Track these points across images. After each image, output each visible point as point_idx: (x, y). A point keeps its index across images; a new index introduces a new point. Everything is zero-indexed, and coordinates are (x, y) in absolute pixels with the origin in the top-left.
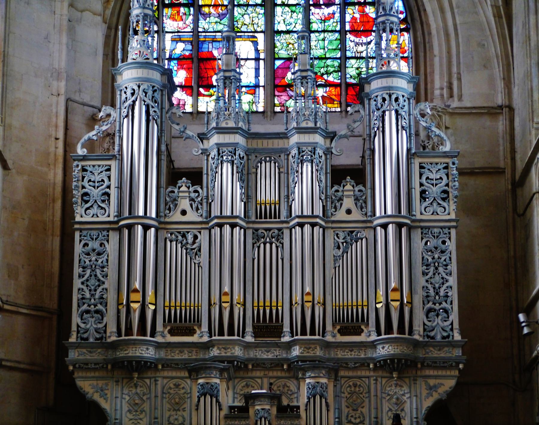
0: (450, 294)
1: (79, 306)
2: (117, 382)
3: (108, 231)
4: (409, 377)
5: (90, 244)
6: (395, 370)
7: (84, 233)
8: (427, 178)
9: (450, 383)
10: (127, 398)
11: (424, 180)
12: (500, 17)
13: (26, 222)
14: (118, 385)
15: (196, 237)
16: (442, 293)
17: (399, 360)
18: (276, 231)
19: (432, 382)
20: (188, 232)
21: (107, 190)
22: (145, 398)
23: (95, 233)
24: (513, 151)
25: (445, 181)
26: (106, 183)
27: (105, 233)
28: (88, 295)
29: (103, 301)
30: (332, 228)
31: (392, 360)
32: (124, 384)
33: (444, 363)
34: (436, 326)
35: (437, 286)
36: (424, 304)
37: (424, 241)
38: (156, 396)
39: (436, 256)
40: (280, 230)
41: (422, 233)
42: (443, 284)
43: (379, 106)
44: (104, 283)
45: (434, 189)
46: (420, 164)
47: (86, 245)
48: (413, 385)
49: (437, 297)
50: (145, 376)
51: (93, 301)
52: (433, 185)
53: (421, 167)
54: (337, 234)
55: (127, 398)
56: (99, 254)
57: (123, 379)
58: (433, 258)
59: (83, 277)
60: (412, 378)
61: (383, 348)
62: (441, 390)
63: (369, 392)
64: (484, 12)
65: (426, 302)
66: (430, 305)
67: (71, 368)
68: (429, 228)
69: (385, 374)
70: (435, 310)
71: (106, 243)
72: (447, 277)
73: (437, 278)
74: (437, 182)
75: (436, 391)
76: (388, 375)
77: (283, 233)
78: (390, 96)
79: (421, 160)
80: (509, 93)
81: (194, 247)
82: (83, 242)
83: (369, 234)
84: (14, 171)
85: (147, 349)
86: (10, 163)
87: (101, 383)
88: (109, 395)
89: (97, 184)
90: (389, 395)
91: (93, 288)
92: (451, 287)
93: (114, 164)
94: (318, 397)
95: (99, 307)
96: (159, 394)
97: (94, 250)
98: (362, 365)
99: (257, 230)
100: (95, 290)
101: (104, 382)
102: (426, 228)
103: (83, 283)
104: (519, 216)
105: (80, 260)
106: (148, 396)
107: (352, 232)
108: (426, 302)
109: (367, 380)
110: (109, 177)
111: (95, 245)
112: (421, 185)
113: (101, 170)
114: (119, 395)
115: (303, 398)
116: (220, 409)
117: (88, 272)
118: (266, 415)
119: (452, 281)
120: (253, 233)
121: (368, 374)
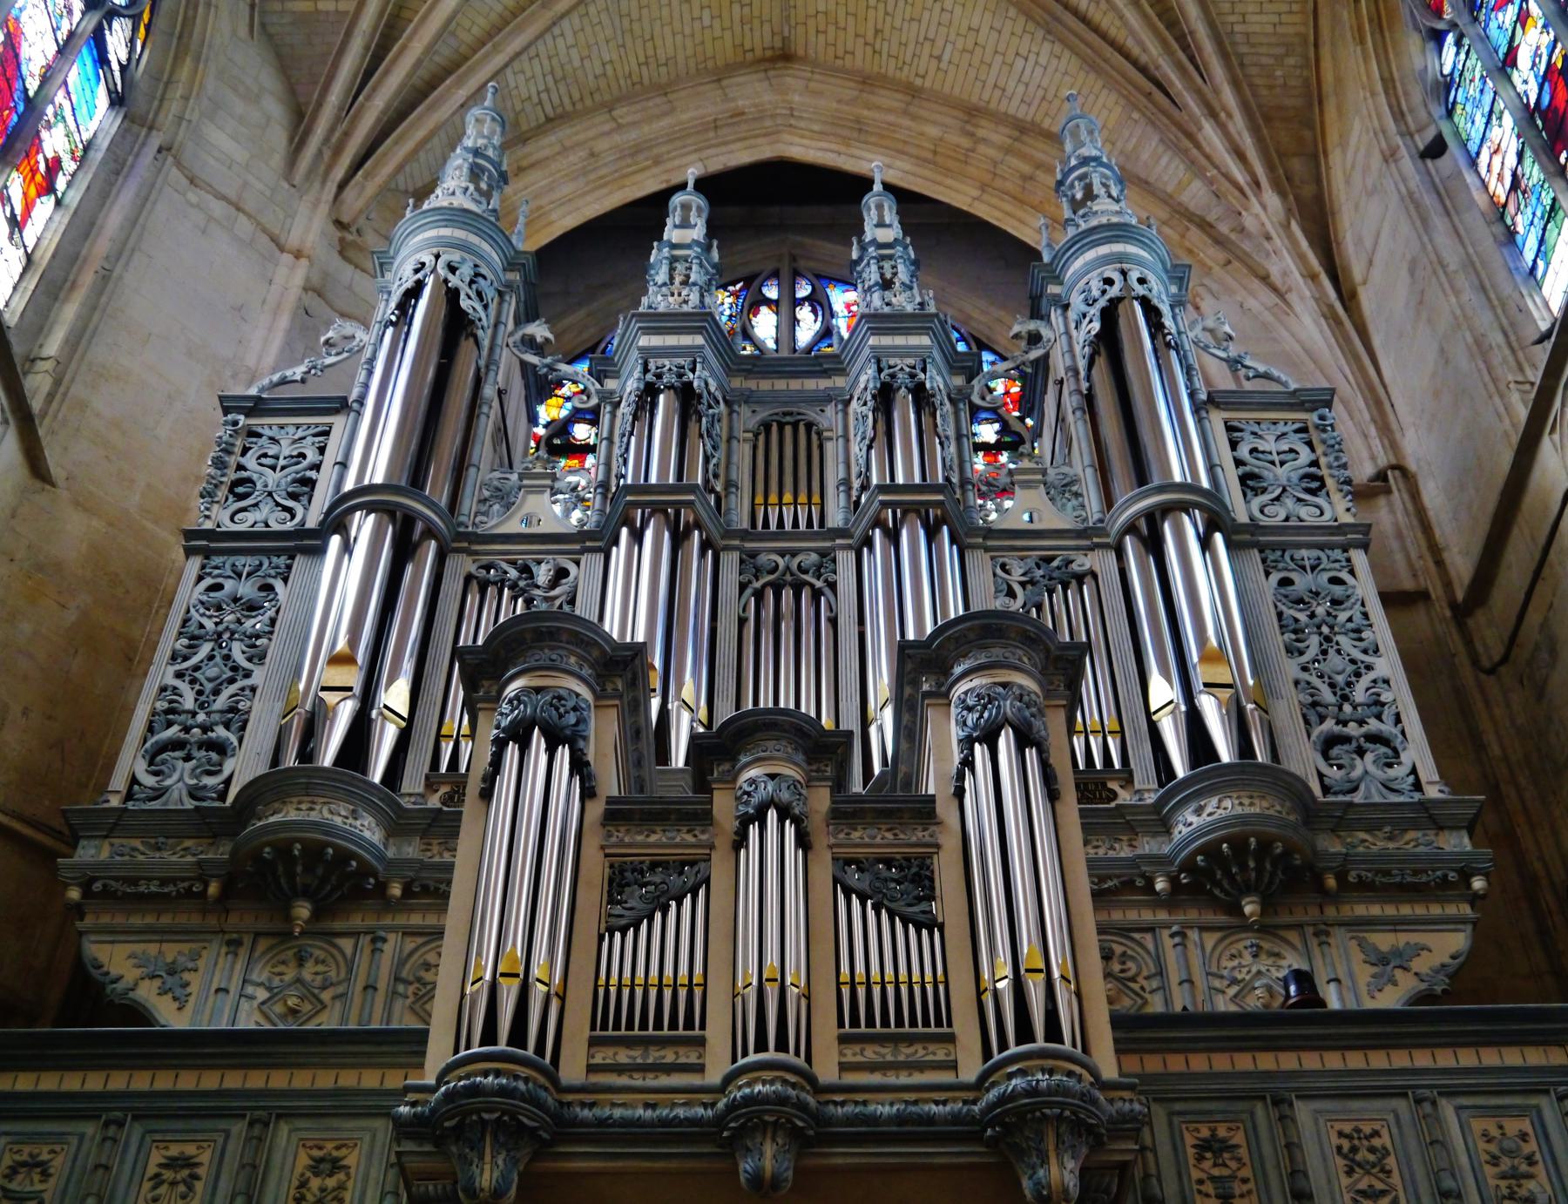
0: (1386, 697)
1: (151, 729)
2: (234, 945)
3: (292, 558)
4: (1299, 927)
5: (229, 585)
6: (1247, 889)
7: (217, 560)
8: (1253, 451)
9: (1450, 945)
10: (262, 994)
11: (1243, 451)
12: (1338, 322)
13: (71, 616)
14: (236, 955)
15: (561, 573)
16: (1359, 695)
17: (1265, 845)
18: (814, 557)
19: (1384, 941)
20: (539, 562)
21: (312, 474)
22: (326, 996)
23: (246, 563)
24: (1435, 550)
25: (1305, 455)
26: (312, 456)
27: (282, 561)
28: (189, 702)
29: (236, 718)
30: (987, 549)
31: (1239, 843)
32: (257, 954)
33: (1416, 873)
34: (1361, 779)
35: (1340, 679)
36: (1307, 722)
37: (1275, 577)
38: (370, 987)
39: (1320, 611)
40: (823, 554)
41: (1264, 561)
42: (1358, 675)
43: (1096, 293)
44: (248, 674)
45: (1279, 471)
46: (1226, 423)
47: (218, 587)
48: (1316, 951)
49: (1347, 708)
50: (338, 925)
51: (201, 717)
52: (1273, 463)
53: (1230, 429)
54: (1003, 567)
55: (262, 994)
56: (252, 608)
57: (257, 935)
58: (1312, 616)
59: (186, 659)
60: (1310, 930)
61: (1199, 811)
62: (1422, 964)
63: (1161, 972)
64: (1293, 335)
65: (1313, 718)
66: (1329, 725)
67: (74, 894)
68: (1283, 548)
69: (1210, 917)
70: (1346, 739)
71: (278, 585)
72: (1368, 659)
73: (1334, 661)
74: (1283, 457)
75: (1406, 969)
76: (1222, 919)
77: (834, 561)
78: (1124, 273)
79: (1227, 415)
80: (1394, 446)
81: (552, 593)
82: (208, 581)
83: (1103, 563)
84: (62, 493)
85: (354, 814)
86: (56, 471)
87: (171, 951)
88: (193, 989)
89: (282, 462)
90: (1234, 981)
91: (209, 686)
92: (1386, 682)
93: (339, 423)
94: (1005, 742)
95: (220, 732)
96: (382, 985)
97: (236, 600)
98: (1128, 885)
99: (753, 555)
100: (216, 692)
101: (185, 947)
102: (1274, 547)
103: (179, 675)
104: (1491, 671)
105: (185, 622)
106: (340, 989)
107: (1049, 560)
108: (1313, 718)
109: (1148, 939)
110: (322, 450)
111: (247, 589)
112: (1239, 463)
113: (300, 433)
114: (234, 988)
115: (943, 758)
116: (588, 793)
117: (206, 649)
118: (785, 796)
119: (1388, 664)
120: (742, 561)
121: (1147, 916)
